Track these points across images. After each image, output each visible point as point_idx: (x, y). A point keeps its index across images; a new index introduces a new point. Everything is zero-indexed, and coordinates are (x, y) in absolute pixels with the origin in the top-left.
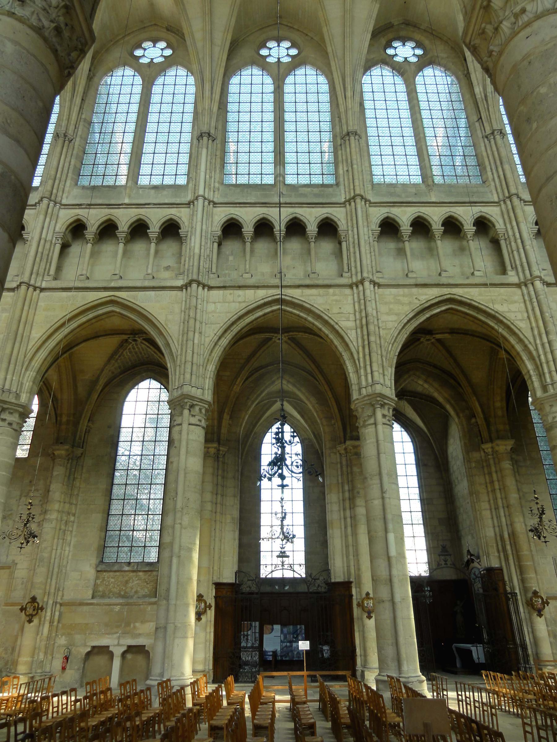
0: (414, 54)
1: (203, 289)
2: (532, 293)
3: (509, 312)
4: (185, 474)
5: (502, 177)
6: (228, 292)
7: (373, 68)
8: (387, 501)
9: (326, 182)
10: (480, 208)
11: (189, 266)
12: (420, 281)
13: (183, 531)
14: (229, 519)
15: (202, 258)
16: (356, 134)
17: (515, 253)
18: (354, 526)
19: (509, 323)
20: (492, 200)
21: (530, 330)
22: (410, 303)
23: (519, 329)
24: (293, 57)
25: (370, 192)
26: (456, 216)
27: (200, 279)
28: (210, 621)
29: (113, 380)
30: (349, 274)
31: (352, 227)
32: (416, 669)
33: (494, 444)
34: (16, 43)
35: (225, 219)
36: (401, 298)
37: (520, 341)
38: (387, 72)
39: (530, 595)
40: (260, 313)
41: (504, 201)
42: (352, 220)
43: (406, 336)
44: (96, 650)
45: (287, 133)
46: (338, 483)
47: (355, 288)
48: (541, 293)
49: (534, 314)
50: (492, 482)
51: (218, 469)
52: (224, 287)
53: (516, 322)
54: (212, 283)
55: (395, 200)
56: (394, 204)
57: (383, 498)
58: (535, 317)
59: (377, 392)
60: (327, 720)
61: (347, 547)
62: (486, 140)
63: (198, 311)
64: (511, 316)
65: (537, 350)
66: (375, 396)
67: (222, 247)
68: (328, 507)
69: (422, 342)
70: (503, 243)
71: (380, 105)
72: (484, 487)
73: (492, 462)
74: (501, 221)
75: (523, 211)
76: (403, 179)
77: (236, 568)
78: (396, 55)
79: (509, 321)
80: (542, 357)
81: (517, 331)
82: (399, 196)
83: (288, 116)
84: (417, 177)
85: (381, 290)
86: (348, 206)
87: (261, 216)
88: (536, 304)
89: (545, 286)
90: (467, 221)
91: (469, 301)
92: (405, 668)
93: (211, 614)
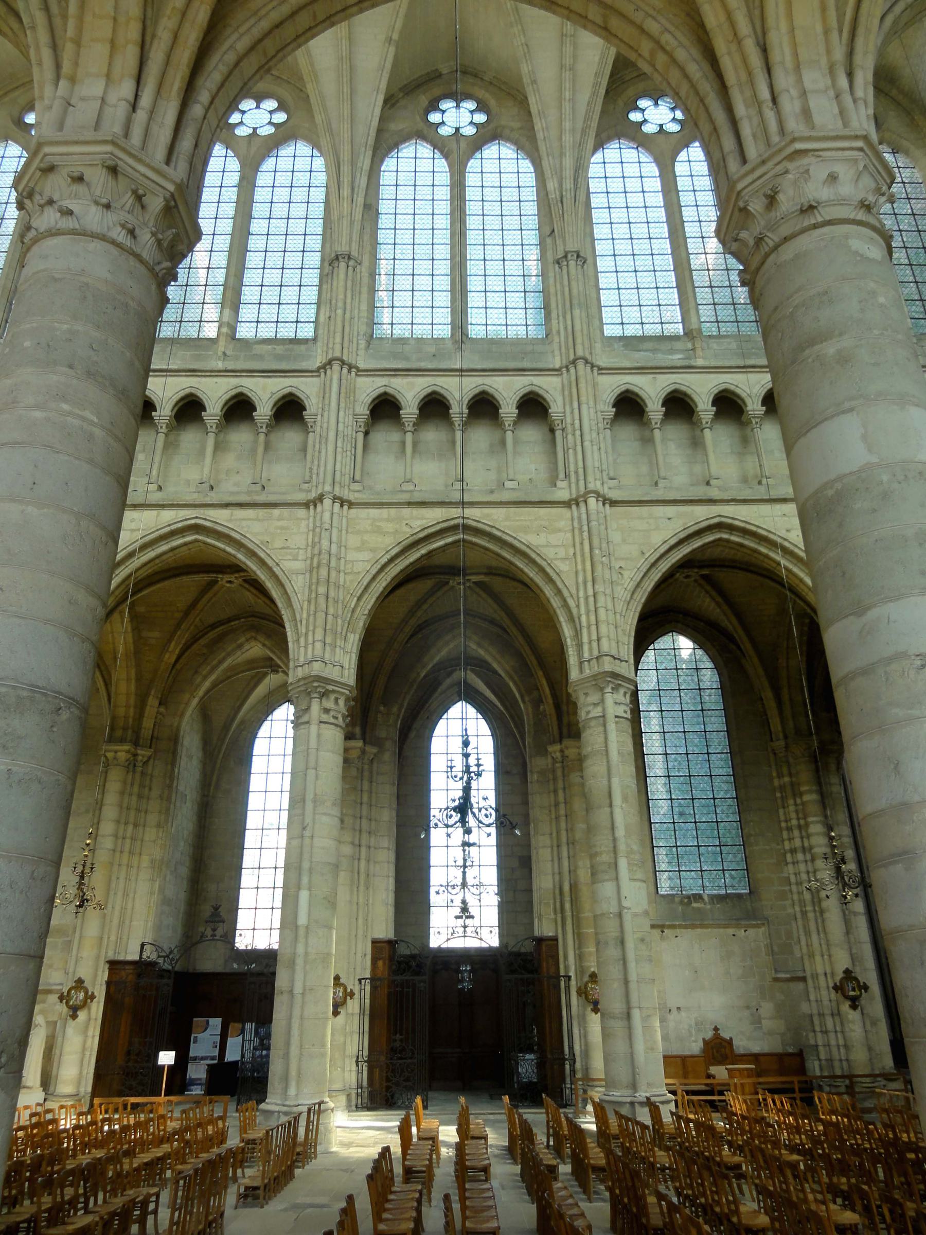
0: (471, 122)
2: (584, 516)
3: (547, 546)
5: (570, 328)
7: (403, 146)
9: (301, 335)
10: (532, 378)
12: (417, 497)
14: (145, 861)
16: (349, 258)
17: (571, 451)
19: (544, 564)
20: (551, 366)
21: (573, 575)
23: (558, 574)
24: (277, 126)
25: (361, 352)
26: (491, 391)
28: (96, 1019)
33: (563, 746)
36: (382, 524)
37: (559, 592)
38: (425, 150)
39: (586, 979)
40: (164, 548)
41: (567, 367)
43: (384, 584)
45: (252, 254)
47: (312, 507)
49: (582, 550)
50: (557, 805)
51: (132, 785)
53: (555, 562)
55: (400, 366)
56: (396, 372)
58: (583, 555)
59: (313, 673)
62: (557, 266)
64: (549, 553)
65: (578, 606)
66: (310, 679)
69: (453, 587)
70: (558, 434)
71: (405, 207)
72: (547, 812)
73: (559, 773)
74: (560, 400)
75: (595, 385)
76: (422, 331)
78: (443, 123)
79: (545, 560)
80: (584, 618)
81: (554, 576)
82: (407, 359)
83: (256, 226)
84: (445, 327)
85: (353, 511)
87: (188, 391)
88: (586, 534)
89: (607, 506)
90: (508, 400)
91: (488, 529)
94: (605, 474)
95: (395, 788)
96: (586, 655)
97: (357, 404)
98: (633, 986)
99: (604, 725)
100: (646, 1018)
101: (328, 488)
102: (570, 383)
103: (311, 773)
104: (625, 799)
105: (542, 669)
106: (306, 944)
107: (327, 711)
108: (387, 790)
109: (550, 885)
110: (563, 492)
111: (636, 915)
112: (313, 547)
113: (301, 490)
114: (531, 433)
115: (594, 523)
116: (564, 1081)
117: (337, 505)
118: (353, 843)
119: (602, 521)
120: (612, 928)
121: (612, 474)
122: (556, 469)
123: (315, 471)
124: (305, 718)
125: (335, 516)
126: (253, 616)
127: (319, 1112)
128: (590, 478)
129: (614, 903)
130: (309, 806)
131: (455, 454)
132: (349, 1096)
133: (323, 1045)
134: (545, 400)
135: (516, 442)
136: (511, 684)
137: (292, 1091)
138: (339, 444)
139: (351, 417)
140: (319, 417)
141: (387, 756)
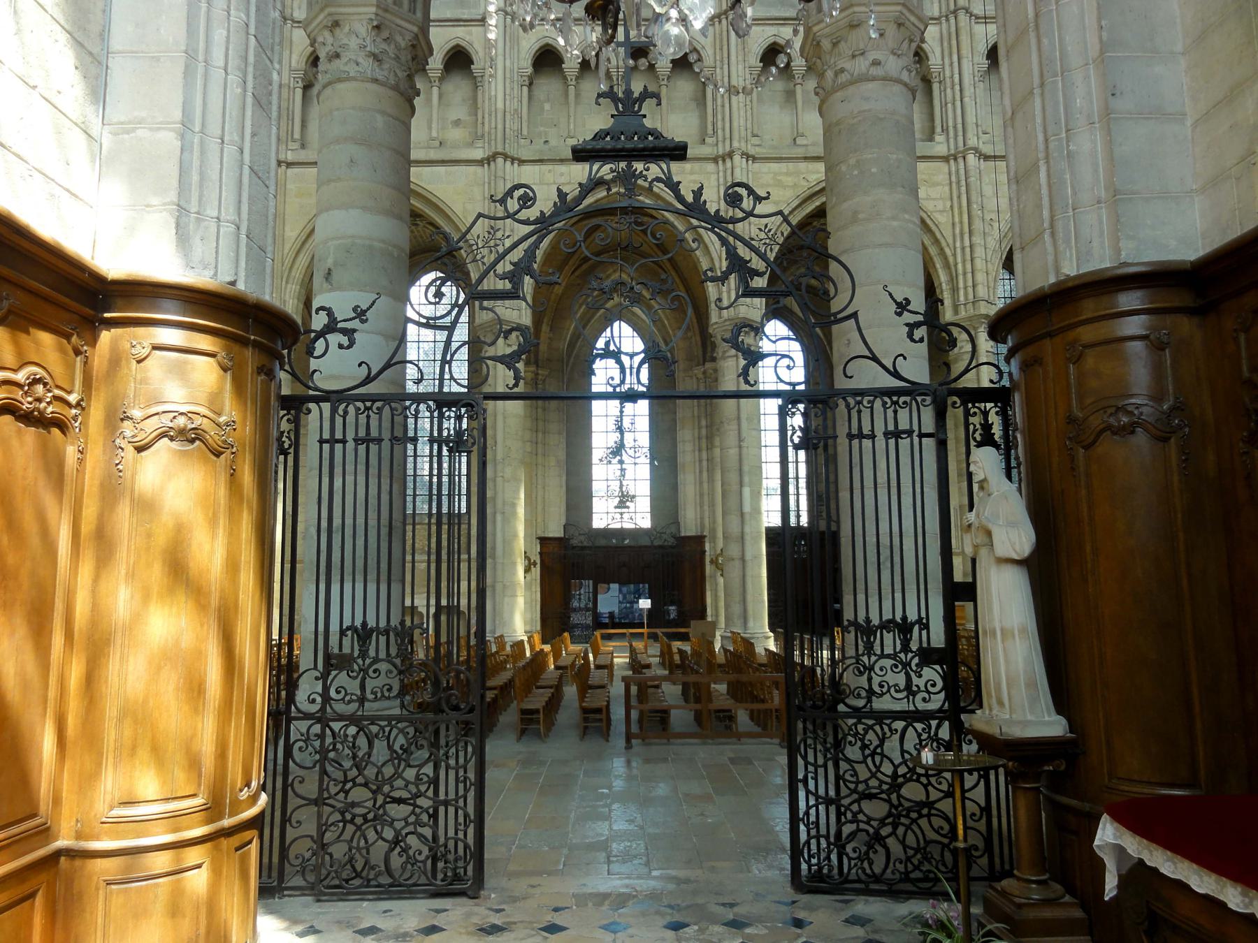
1: (512, 164)
2: (962, 172)
3: (927, 199)
4: (505, 418)
6: (545, 168)
8: (744, 451)
11: (490, 128)
13: (506, 484)
14: (553, 463)
17: (949, 105)
18: (711, 471)
27: (507, 150)
30: (714, 139)
31: (722, 61)
32: (763, 627)
34: (383, 113)
35: (536, 47)
41: (947, 16)
42: (721, 49)
46: (693, 416)
47: (720, 162)
48: (972, 173)
52: (541, 161)
57: (740, 447)
58: (960, 207)
60: (665, 669)
61: (701, 495)
65: (954, 255)
67: (533, 87)
68: (680, 447)
70: (936, 87)
77: (563, 521)
80: (960, 266)
81: (934, 228)
85: (756, 165)
86: (717, 23)
88: (963, 189)
92: (751, 624)
93: (536, 571)
94: (980, 128)
102: (950, 34)
122: (932, 119)
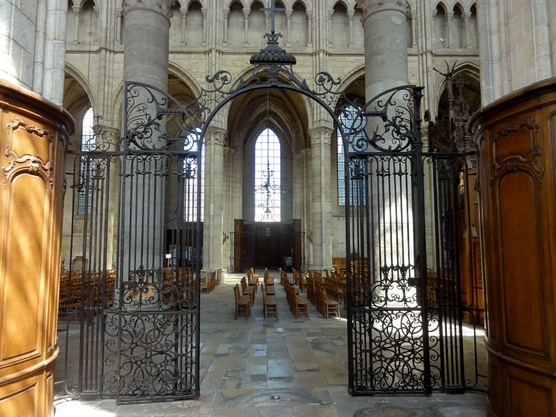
2: (318, 61)
3: (302, 73)
15: (109, 30)
17: (314, 30)
21: (312, 86)
22: (242, 66)
29: (73, 105)
36: (236, 62)
39: (310, 233)
44: (79, 258)
47: (207, 54)
48: (321, 61)
50: (303, 172)
54: (116, 49)
63: (107, 69)
70: (310, 21)
73: (304, 160)
74: (311, 6)
85: (224, 56)
94: (327, 41)
95: (242, 165)
96: (315, 119)
97: (224, 5)
98: (324, 236)
99: (320, 147)
100: (327, 246)
101: (213, 46)
103: (212, 163)
104: (326, 174)
105: (299, 119)
106: (213, 222)
107: (217, 139)
108: (238, 166)
109: (299, 201)
110: (310, 50)
111: (326, 213)
112: (209, 72)
113: (202, 46)
114: (298, 19)
115: (321, 64)
116: (301, 266)
117: (218, 54)
118: (226, 186)
119: (325, 63)
120: (318, 217)
121: (330, 41)
123: (208, 37)
124: (209, 142)
125: (217, 59)
126: (182, 94)
127: (221, 272)
128: (321, 44)
129: (319, 209)
130: (212, 175)
131: (266, 29)
132: (228, 269)
133: (220, 253)
134: (304, 4)
135: (291, 23)
136: (287, 125)
137: (211, 266)
138: (217, 25)
139: (222, 11)
140: (208, 11)
141: (239, 153)
